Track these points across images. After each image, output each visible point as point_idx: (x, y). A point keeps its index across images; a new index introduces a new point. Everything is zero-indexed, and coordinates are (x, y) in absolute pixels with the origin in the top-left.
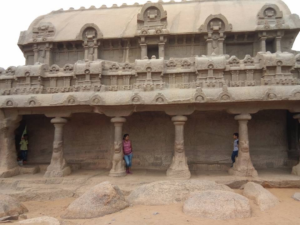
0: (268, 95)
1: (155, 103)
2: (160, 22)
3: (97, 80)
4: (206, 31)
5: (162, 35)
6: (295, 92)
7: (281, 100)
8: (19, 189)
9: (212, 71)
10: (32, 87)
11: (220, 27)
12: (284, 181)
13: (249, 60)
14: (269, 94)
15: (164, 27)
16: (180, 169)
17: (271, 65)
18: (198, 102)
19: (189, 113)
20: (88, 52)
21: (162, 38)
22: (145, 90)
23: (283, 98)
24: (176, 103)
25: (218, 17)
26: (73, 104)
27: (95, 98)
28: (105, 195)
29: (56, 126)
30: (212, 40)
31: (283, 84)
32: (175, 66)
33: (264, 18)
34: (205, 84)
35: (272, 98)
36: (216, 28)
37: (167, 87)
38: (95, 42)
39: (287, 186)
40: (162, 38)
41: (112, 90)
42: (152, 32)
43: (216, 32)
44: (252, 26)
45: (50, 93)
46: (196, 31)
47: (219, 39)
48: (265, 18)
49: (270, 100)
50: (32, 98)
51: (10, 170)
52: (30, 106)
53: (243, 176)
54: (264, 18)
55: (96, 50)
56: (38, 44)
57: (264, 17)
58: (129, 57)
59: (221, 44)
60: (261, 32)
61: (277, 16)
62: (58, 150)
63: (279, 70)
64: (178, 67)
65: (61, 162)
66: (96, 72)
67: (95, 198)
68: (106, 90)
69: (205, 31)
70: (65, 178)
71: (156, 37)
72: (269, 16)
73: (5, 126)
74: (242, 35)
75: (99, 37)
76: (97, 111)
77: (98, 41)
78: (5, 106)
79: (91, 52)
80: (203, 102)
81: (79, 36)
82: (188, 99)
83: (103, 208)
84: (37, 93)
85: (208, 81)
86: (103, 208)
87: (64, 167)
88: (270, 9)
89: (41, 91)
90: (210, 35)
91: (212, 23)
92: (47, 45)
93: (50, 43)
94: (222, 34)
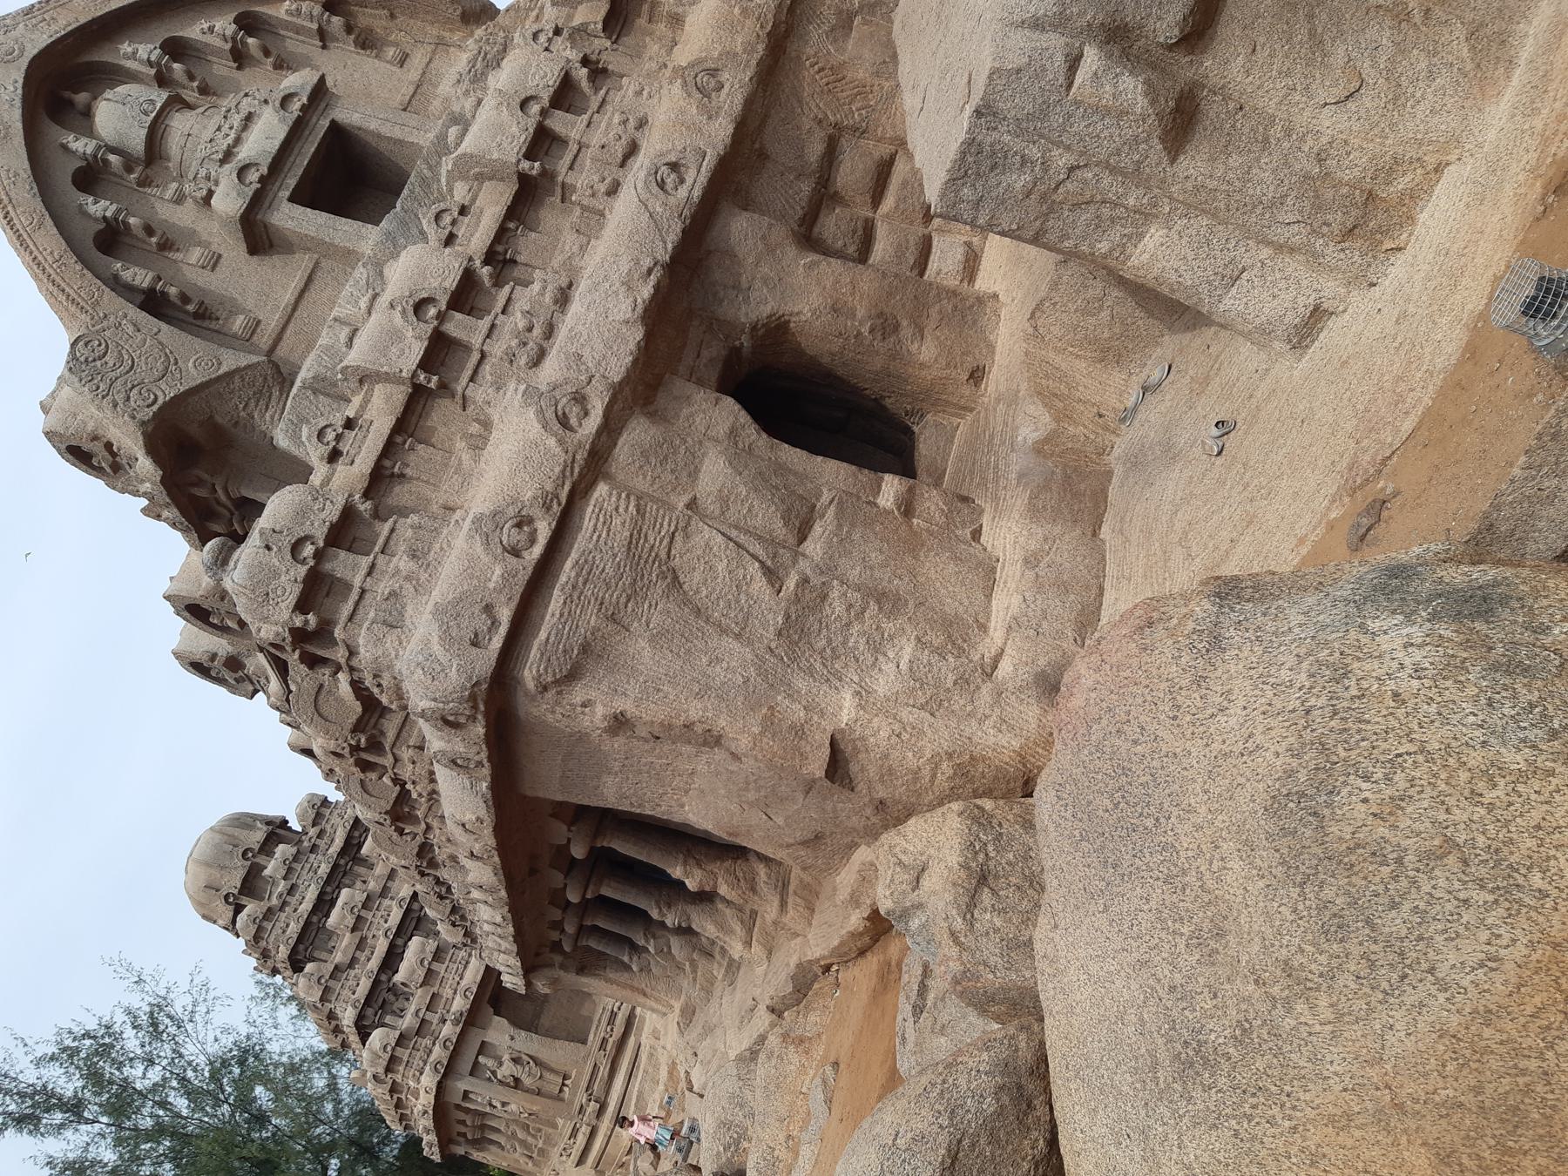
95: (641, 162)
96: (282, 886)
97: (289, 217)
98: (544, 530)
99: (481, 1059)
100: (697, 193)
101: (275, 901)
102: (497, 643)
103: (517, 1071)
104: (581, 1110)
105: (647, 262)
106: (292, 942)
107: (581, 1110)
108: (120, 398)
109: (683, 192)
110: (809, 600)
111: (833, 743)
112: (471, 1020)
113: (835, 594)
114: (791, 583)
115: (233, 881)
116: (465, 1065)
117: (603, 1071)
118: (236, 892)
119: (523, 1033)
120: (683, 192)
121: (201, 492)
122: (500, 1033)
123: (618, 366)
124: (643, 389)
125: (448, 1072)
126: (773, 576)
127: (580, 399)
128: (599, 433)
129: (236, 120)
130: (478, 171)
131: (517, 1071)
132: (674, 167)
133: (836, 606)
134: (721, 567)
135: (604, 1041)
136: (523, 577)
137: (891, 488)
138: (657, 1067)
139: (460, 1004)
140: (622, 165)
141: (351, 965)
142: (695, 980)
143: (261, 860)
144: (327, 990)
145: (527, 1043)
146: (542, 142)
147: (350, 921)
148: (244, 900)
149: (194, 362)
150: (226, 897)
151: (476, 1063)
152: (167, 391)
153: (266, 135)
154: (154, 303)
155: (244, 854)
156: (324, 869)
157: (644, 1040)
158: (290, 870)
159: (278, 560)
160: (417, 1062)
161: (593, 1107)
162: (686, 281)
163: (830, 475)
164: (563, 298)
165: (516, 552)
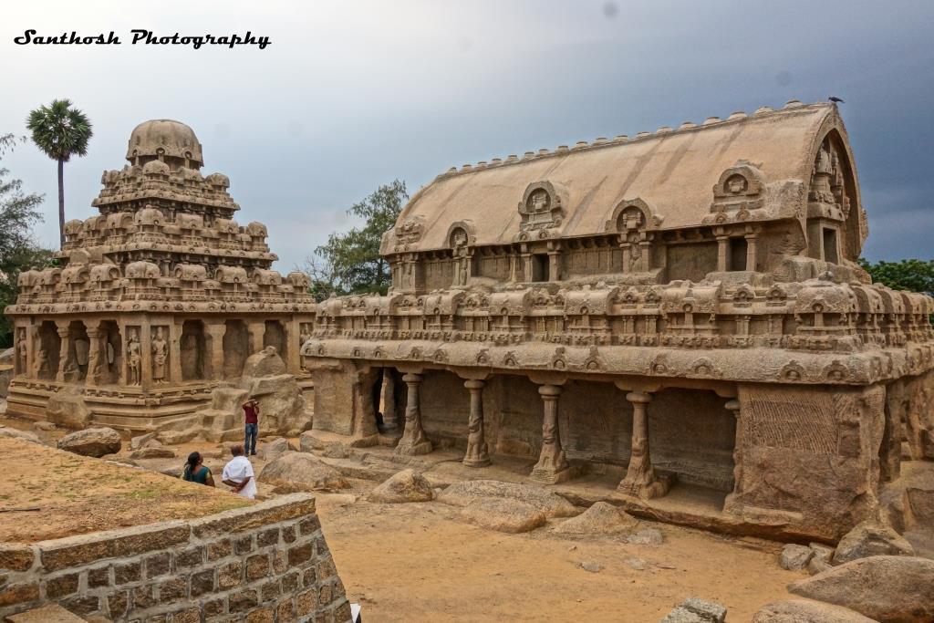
0: (654, 367)
1: (504, 366)
2: (550, 214)
3: (449, 324)
4: (616, 232)
5: (549, 240)
6: (698, 364)
7: (674, 376)
8: (364, 464)
9: (587, 318)
10: (382, 331)
11: (639, 222)
12: (676, 513)
13: (652, 297)
14: (656, 365)
15: (555, 224)
16: (545, 468)
17: (675, 311)
18: (558, 369)
19: (560, 383)
20: (460, 266)
21: (550, 245)
22: (497, 344)
23: (678, 373)
24: (530, 368)
25: (634, 205)
26: (418, 360)
27: (439, 353)
28: (400, 484)
29: (409, 385)
30: (628, 245)
31: (691, 347)
32: (545, 304)
33: (724, 197)
34: (574, 340)
35: (661, 373)
36: (631, 224)
37: (529, 337)
38: (467, 250)
39: (682, 522)
40: (550, 245)
41: (465, 339)
42: (533, 236)
43: (632, 232)
44: (700, 216)
45: (402, 339)
46: (601, 231)
47: (641, 244)
48: (728, 195)
49: (657, 374)
50: (378, 347)
51: (366, 438)
52: (377, 358)
53: (625, 493)
54: (724, 197)
55: (469, 263)
56: (402, 255)
57: (724, 195)
58: (516, 270)
59: (645, 252)
60: (715, 227)
61: (747, 193)
62: (411, 419)
63: (689, 318)
64: (550, 305)
65: (415, 435)
66: (446, 312)
67: (392, 485)
68: (458, 338)
69: (614, 231)
70: (414, 458)
71: (542, 243)
72: (734, 193)
73: (358, 381)
74: (686, 232)
75: (470, 244)
76: (448, 369)
77: (470, 249)
78: (353, 357)
79: (463, 266)
80: (563, 370)
81: (445, 242)
82: (545, 363)
83: (395, 496)
84: (387, 338)
85: (580, 334)
86: (395, 496)
87: (419, 442)
88: (735, 177)
89: (390, 335)
90: (624, 237)
91: (625, 216)
92: (411, 257)
93: (414, 253)
94: (643, 235)
96: (180, 179)
99: (160, 329)
101: (172, 178)
104: (152, 395)
106: (161, 197)
107: (152, 395)
112: (178, 315)
115: (173, 151)
116: (156, 322)
117: (175, 398)
118: (166, 154)
119: (179, 346)
121: (748, 229)
122: (176, 332)
125: (150, 314)
131: (161, 351)
135: (189, 392)
138: (189, 426)
139: (186, 306)
141: (167, 235)
142: (417, 444)
143: (187, 163)
144: (151, 227)
145: (175, 349)
147: (188, 226)
148: (161, 158)
150: (161, 149)
156: (199, 200)
157: (198, 413)
158: (191, 181)
160: (150, 294)
161: (157, 401)
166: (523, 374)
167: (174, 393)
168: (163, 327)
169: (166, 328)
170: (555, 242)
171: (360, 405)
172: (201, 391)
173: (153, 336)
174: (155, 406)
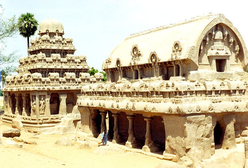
29: (102, 116)
95: (236, 103)
96: (54, 41)
97: (214, 62)
98: (200, 112)
99: (42, 96)
100: (236, 111)
102: (189, 113)
103: (42, 104)
104: (39, 120)
105: (227, 110)
106: (46, 48)
107: (39, 120)
108: (190, 54)
109: (235, 110)
110: (201, 140)
111: (190, 149)
112: (49, 91)
113: (203, 143)
114: (202, 138)
116: (41, 94)
118: (49, 32)
119: (49, 102)
120: (235, 110)
123: (216, 112)
124: (214, 115)
126: (202, 136)
127: (212, 109)
128: (210, 113)
129: (222, 48)
130: (229, 85)
131: (42, 104)
132: (238, 108)
133: (202, 143)
134: (201, 130)
135: (53, 119)
136: (195, 112)
137: (213, 144)
138: (52, 131)
139: (51, 88)
140: (235, 101)
146: (235, 91)
147: (55, 59)
149: (195, 60)
150: (48, 30)
151: (41, 96)
152: (192, 59)
153: (222, 53)
154: (200, 50)
155: (57, 30)
156: (60, 48)
159: (187, 88)
160: (38, 84)
161: (41, 122)
162: (227, 116)
163: (212, 137)
164: (220, 102)
165: (197, 111)
166: (141, 113)
167: (47, 119)
168: (43, 95)
169: (44, 96)
170: (138, 66)
171: (91, 122)
172: (57, 119)
173: (40, 99)
174: (41, 124)
